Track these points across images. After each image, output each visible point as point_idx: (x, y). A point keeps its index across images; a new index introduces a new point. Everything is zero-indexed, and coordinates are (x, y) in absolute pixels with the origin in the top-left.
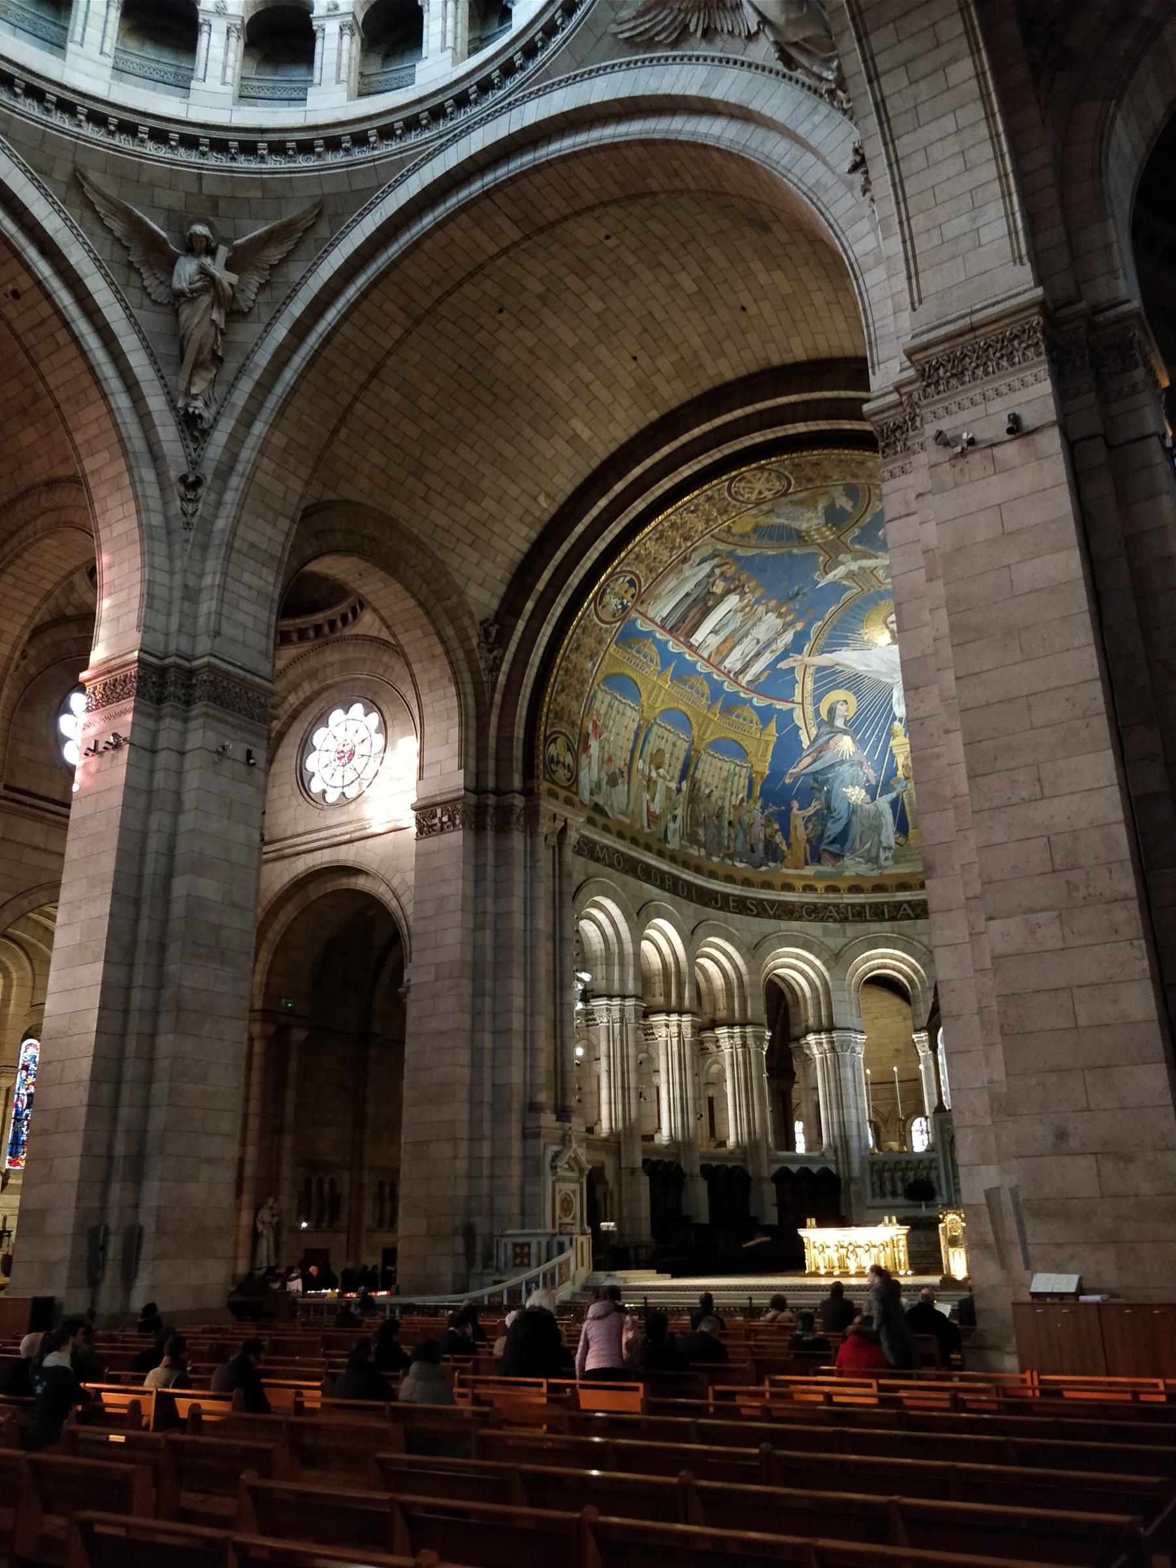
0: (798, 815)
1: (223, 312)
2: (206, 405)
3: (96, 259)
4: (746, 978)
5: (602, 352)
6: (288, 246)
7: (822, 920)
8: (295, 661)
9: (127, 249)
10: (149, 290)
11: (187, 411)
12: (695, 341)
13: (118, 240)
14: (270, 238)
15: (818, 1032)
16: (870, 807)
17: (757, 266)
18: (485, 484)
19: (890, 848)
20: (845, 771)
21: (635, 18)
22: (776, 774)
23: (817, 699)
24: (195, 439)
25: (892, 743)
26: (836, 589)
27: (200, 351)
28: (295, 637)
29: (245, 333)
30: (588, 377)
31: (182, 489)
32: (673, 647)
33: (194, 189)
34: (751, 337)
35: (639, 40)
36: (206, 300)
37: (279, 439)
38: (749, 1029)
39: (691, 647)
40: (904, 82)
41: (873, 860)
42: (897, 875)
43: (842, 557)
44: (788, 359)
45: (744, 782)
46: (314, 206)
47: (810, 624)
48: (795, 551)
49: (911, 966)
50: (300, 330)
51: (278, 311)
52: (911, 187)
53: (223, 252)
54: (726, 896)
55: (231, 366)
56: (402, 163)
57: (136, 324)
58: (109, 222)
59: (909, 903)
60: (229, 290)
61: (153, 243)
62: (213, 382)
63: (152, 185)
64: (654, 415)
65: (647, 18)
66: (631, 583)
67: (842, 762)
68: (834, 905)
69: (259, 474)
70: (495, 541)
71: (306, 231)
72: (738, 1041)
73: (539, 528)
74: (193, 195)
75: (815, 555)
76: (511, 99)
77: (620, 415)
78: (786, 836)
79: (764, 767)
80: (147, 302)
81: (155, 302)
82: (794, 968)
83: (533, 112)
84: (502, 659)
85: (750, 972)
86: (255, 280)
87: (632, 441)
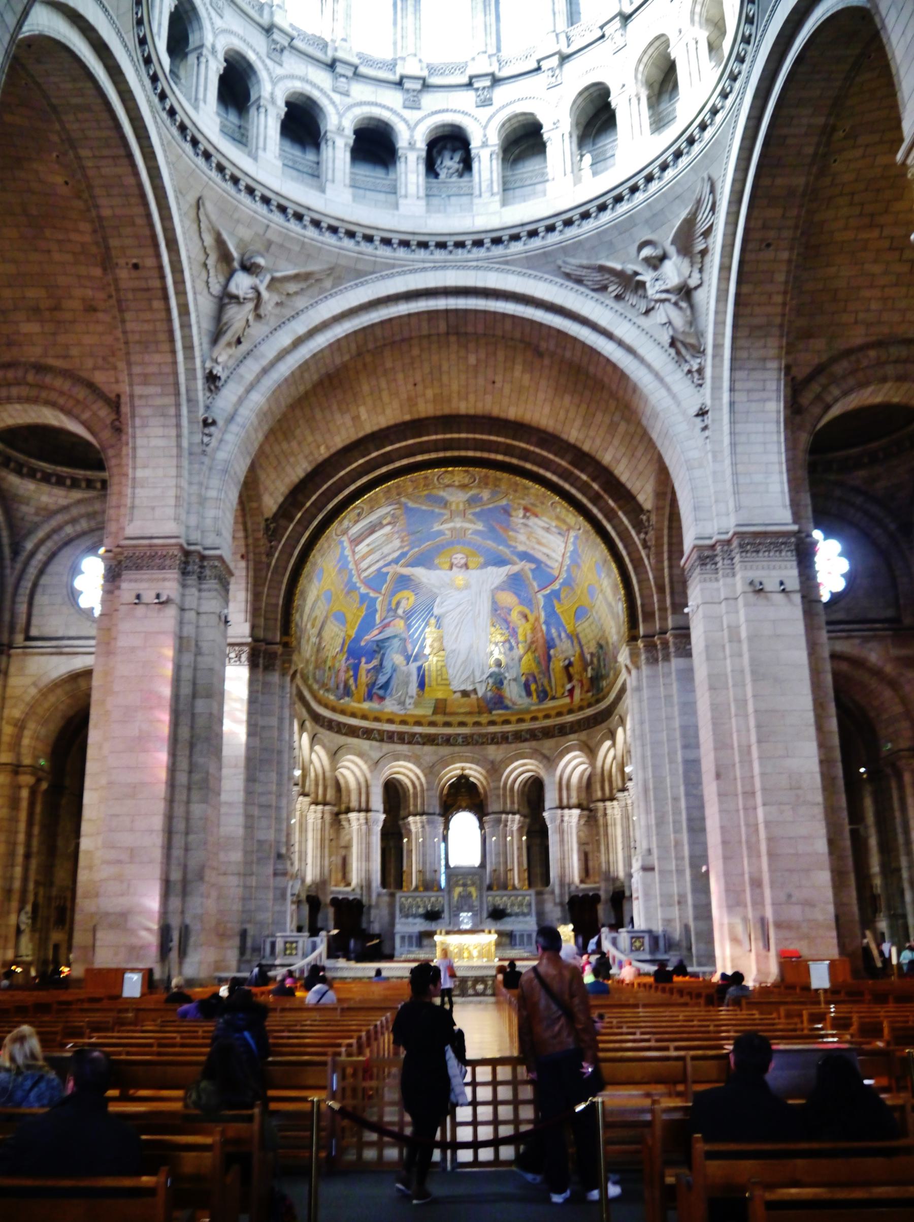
0: (364, 667)
4: (328, 774)
5: (400, 376)
6: (303, 285)
7: (368, 739)
8: (79, 502)
9: (207, 255)
11: (211, 372)
12: (455, 387)
13: (205, 248)
14: (296, 277)
15: (359, 811)
16: (404, 669)
17: (518, 368)
18: (298, 432)
19: (412, 697)
20: (396, 643)
22: (357, 639)
23: (393, 594)
24: (210, 390)
25: (427, 630)
26: (440, 533)
28: (83, 484)
29: (258, 330)
32: (347, 552)
33: (261, 232)
36: (250, 306)
38: (327, 808)
39: (354, 552)
40: (745, 399)
41: (402, 703)
42: (413, 716)
43: (457, 519)
44: (503, 415)
45: (341, 641)
47: (411, 549)
48: (437, 510)
49: (416, 775)
50: (298, 342)
52: (740, 449)
54: (324, 718)
55: (243, 348)
56: (393, 266)
59: (421, 734)
61: (225, 256)
62: (230, 356)
63: (238, 221)
64: (407, 417)
66: (359, 514)
67: (395, 637)
68: (379, 731)
70: (288, 469)
72: (320, 815)
73: (314, 465)
75: (443, 515)
76: (480, 264)
77: (388, 411)
78: (356, 680)
79: (353, 633)
80: (206, 291)
82: (348, 768)
83: (492, 280)
84: (276, 548)
85: (428, 783)
87: (388, 428)
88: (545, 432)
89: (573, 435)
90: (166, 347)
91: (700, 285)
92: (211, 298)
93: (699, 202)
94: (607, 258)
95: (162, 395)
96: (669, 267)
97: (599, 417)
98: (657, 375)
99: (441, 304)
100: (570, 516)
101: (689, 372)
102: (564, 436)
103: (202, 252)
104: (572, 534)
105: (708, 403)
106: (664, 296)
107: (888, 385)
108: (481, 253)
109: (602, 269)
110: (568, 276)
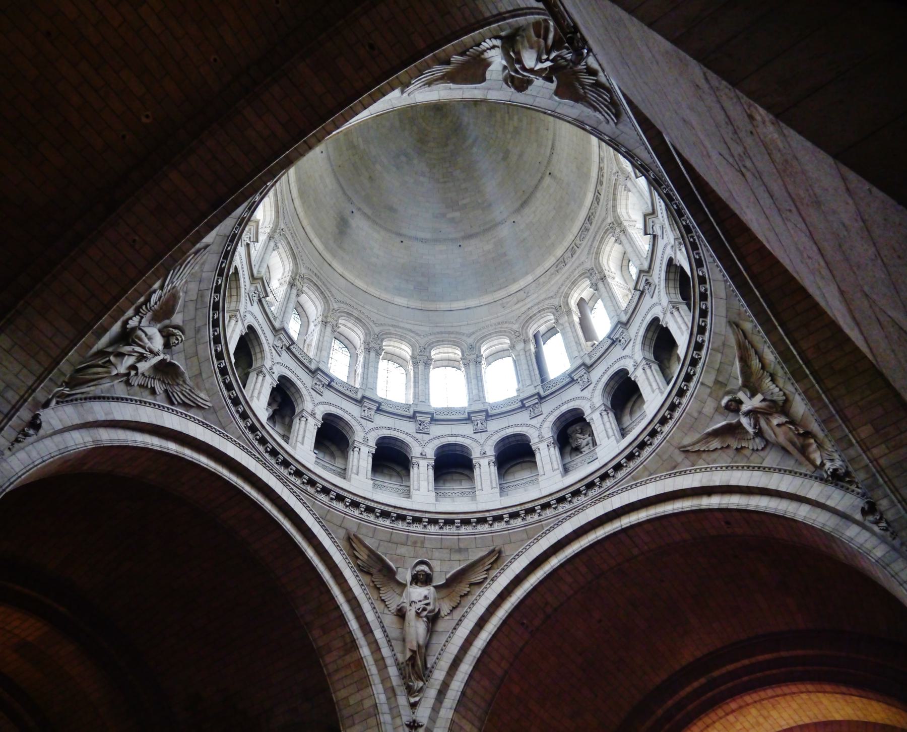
1: (776, 415)
2: (832, 460)
3: (727, 467)
6: (752, 352)
9: (728, 447)
10: (755, 448)
13: (722, 448)
21: (600, 112)
27: (793, 444)
31: (871, 518)
33: (708, 390)
35: (614, 111)
37: (865, 431)
46: (731, 326)
53: (741, 395)
57: (770, 469)
58: (712, 447)
60: (764, 404)
62: (820, 446)
63: (700, 412)
65: (598, 106)
69: (882, 462)
71: (745, 337)
80: (762, 454)
81: (763, 449)
86: (767, 383)
92: (768, 449)
103: (728, 451)
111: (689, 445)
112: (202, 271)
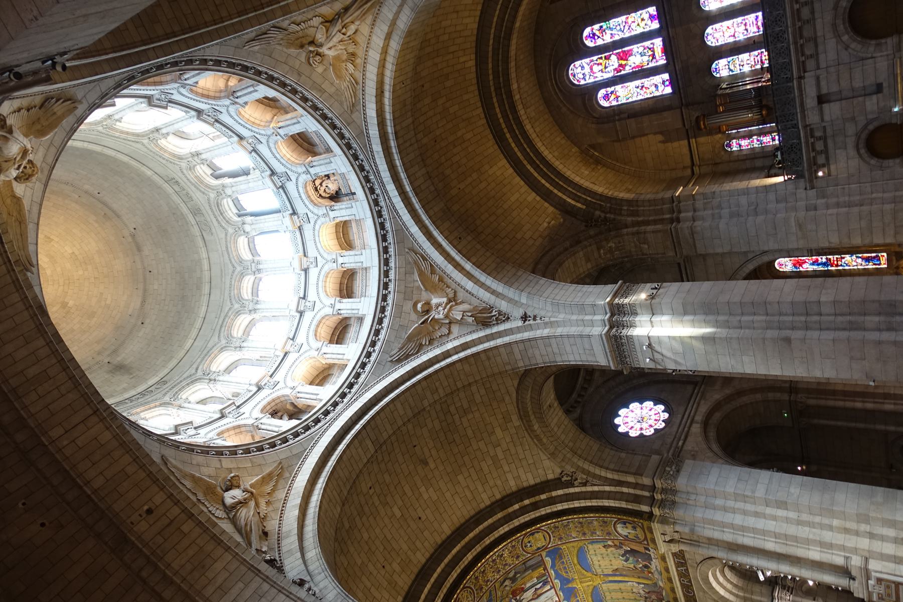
6: (272, 483)
12: (405, 547)
17: (423, 489)
30: (368, 584)
34: (426, 533)
44: (444, 537)
46: (280, 463)
51: (282, 510)
74: (219, 468)
88: (472, 517)
89: (486, 500)
90: (219, 551)
91: (455, 292)
93: (415, 263)
94: (406, 333)
95: (246, 585)
96: (435, 301)
97: (483, 464)
98: (488, 338)
99: (358, 427)
100: (536, 535)
101: (497, 319)
102: (482, 506)
104: (548, 561)
105: (521, 312)
106: (448, 307)
107: (559, 270)
108: (349, 396)
109: (410, 339)
110: (399, 361)
111: (171, 463)
112: (337, 100)
